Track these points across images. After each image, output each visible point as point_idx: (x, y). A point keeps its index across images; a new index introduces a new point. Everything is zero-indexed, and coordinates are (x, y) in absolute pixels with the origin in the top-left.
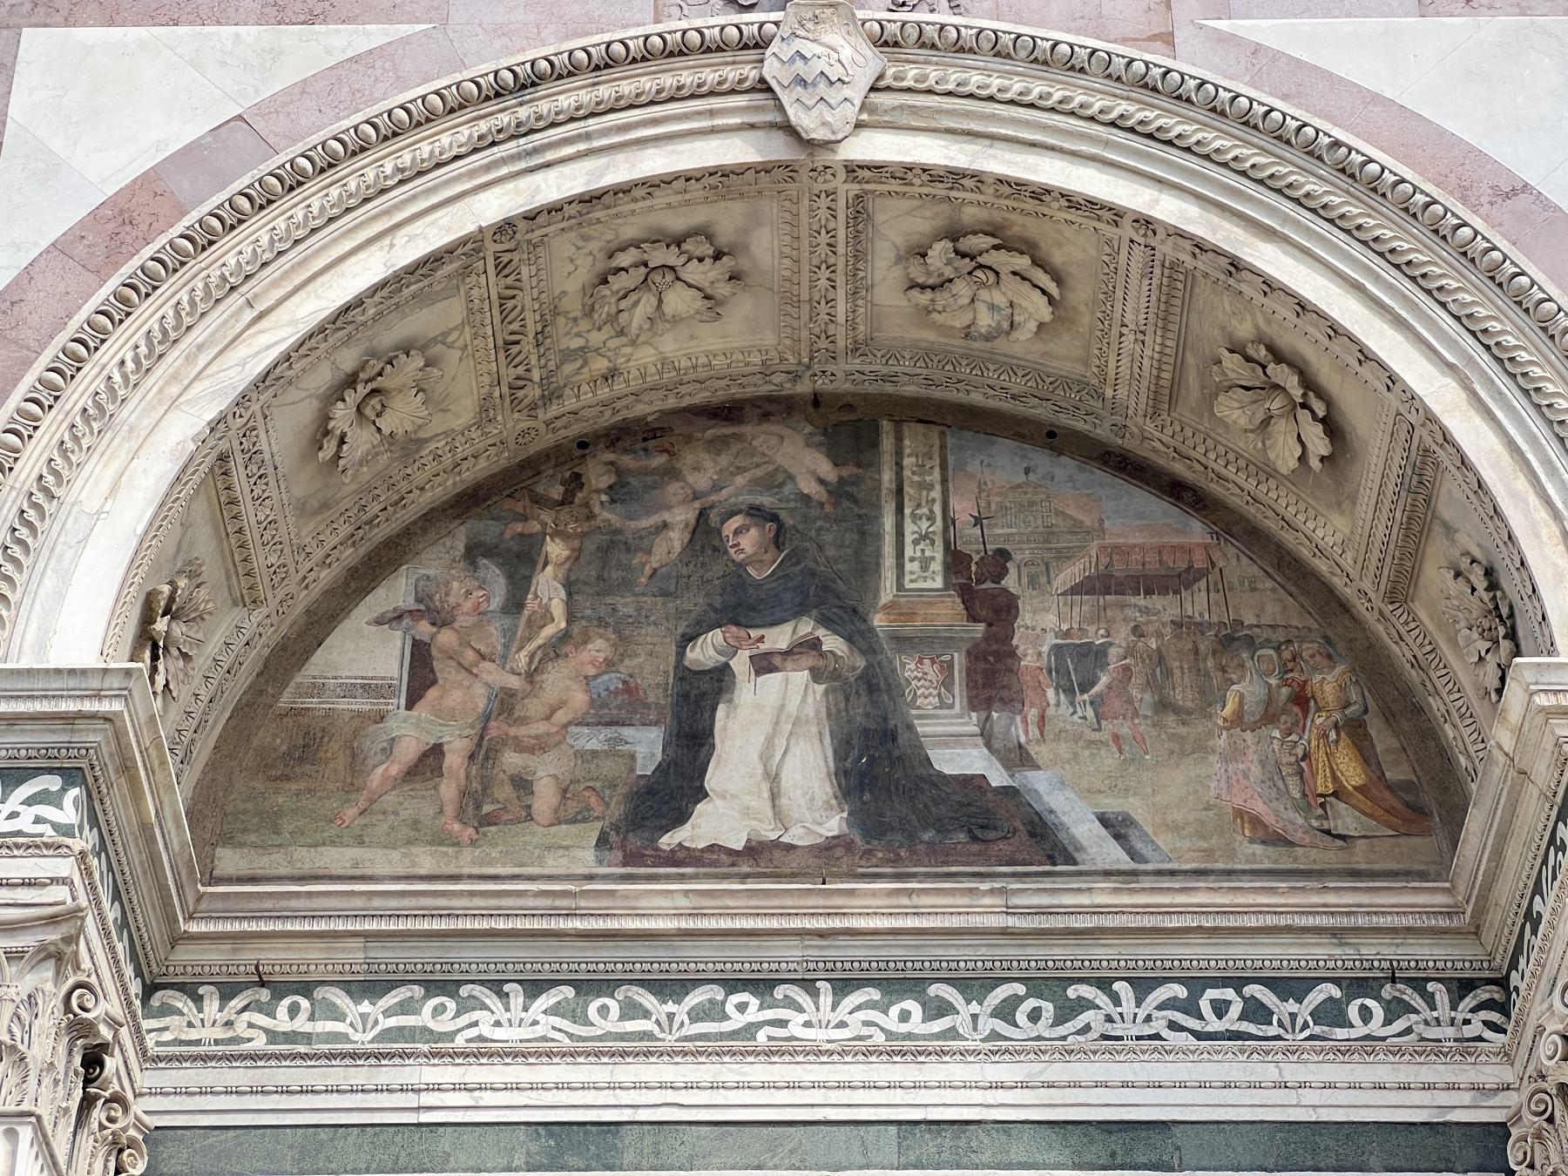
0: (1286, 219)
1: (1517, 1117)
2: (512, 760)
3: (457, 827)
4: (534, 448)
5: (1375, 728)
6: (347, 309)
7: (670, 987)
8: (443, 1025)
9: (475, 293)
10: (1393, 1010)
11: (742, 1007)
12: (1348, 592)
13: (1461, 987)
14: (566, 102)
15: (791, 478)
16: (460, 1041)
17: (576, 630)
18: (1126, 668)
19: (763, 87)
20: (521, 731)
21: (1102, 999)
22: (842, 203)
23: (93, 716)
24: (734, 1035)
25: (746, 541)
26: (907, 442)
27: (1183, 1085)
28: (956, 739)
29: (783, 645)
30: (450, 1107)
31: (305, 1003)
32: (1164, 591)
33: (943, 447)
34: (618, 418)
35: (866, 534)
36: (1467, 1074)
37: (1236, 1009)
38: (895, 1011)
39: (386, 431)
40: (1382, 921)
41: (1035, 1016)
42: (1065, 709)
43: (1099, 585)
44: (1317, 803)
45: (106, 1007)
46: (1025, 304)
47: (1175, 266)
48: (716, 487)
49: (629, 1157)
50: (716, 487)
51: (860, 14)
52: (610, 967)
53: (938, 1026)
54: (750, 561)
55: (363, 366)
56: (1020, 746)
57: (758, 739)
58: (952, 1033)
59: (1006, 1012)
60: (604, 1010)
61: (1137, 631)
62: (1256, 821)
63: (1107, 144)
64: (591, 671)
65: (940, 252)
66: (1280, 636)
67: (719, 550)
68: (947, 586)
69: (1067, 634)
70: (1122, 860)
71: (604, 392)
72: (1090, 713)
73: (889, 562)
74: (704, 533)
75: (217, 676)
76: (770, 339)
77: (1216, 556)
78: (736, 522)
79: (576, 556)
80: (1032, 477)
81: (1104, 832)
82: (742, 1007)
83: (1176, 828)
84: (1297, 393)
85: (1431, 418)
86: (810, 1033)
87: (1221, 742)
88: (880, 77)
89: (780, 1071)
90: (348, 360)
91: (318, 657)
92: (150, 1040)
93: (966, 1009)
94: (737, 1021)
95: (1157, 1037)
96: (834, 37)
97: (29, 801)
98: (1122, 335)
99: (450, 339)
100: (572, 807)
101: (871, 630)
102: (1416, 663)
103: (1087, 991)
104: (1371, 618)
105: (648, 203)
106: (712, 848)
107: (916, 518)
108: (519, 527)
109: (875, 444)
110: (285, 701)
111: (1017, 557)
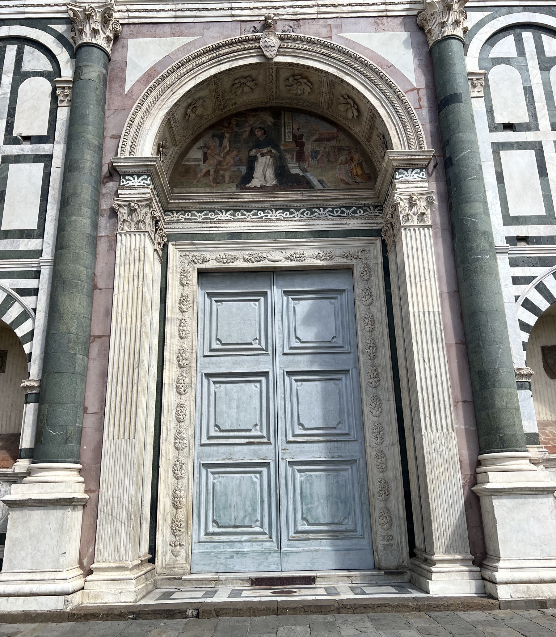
0: (351, 72)
1: (383, 228)
2: (221, 172)
4: (223, 117)
5: (364, 164)
6: (189, 91)
7: (249, 211)
10: (365, 211)
11: (260, 213)
12: (360, 140)
13: (375, 207)
14: (225, 51)
15: (266, 122)
16: (215, 220)
17: (231, 149)
19: (259, 47)
21: (318, 211)
23: (151, 165)
24: (259, 218)
25: (259, 133)
27: (331, 224)
28: (294, 168)
29: (266, 152)
30: (214, 230)
35: (279, 132)
36: (376, 221)
37: (339, 212)
40: (363, 197)
41: (307, 214)
42: (312, 162)
43: (318, 140)
44: (354, 177)
45: (158, 214)
47: (332, 81)
48: (254, 124)
49: (243, 238)
50: (254, 124)
51: (277, 33)
53: (292, 216)
55: (192, 102)
57: (262, 168)
58: (294, 217)
59: (303, 213)
61: (325, 148)
62: (344, 180)
63: (320, 58)
65: (291, 79)
66: (348, 148)
67: (255, 135)
70: (322, 188)
71: (234, 107)
73: (283, 136)
74: (252, 132)
75: (171, 158)
78: (257, 130)
79: (231, 136)
82: (260, 213)
83: (331, 182)
84: (352, 104)
85: (375, 108)
87: (338, 167)
88: (280, 45)
89: (267, 224)
90: (189, 101)
91: (188, 155)
92: (166, 220)
94: (260, 216)
96: (272, 38)
97: (142, 180)
100: (232, 180)
102: (371, 153)
103: (316, 210)
104: (363, 145)
106: (255, 187)
107: (288, 129)
109: (281, 115)
110: (183, 163)
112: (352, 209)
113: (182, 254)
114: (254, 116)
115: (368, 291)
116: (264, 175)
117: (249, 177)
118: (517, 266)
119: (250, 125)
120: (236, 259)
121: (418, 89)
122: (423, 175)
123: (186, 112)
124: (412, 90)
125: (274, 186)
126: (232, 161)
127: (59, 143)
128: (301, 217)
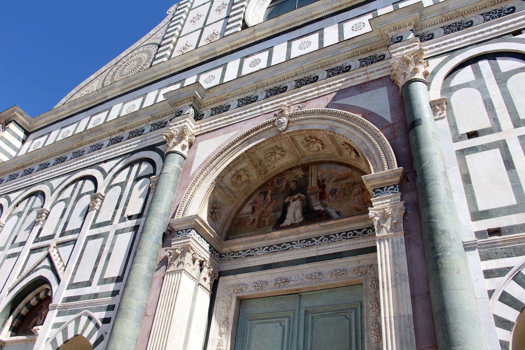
2: (263, 219)
3: (256, 229)
8: (253, 254)
11: (288, 246)
15: (298, 176)
18: (340, 191)
21: (334, 236)
24: (287, 249)
26: (313, 167)
28: (317, 205)
29: (296, 197)
30: (253, 264)
31: (237, 254)
32: (345, 179)
33: (317, 167)
34: (277, 173)
37: (352, 235)
38: (307, 243)
41: (325, 240)
48: (289, 179)
50: (289, 179)
53: (312, 244)
56: (326, 204)
57: (292, 210)
58: (314, 245)
61: (342, 186)
62: (357, 208)
64: (273, 206)
68: (317, 185)
69: (332, 188)
71: (273, 170)
72: (335, 198)
74: (288, 185)
76: (292, 158)
78: (291, 183)
79: (272, 191)
80: (329, 168)
81: (336, 213)
86: (296, 248)
93: (316, 241)
94: (287, 247)
95: (341, 240)
99: (248, 167)
101: (307, 193)
103: (332, 236)
105: (264, 144)
108: (266, 189)
109: (309, 169)
110: (238, 217)
111: (326, 179)
112: (363, 231)
114: (289, 173)
115: (375, 303)
116: (294, 215)
117: (283, 218)
118: (490, 259)
119: (287, 180)
121: (393, 124)
122: (396, 190)
124: (387, 126)
125: (301, 222)
126: (272, 209)
127: (144, 217)
128: (320, 244)
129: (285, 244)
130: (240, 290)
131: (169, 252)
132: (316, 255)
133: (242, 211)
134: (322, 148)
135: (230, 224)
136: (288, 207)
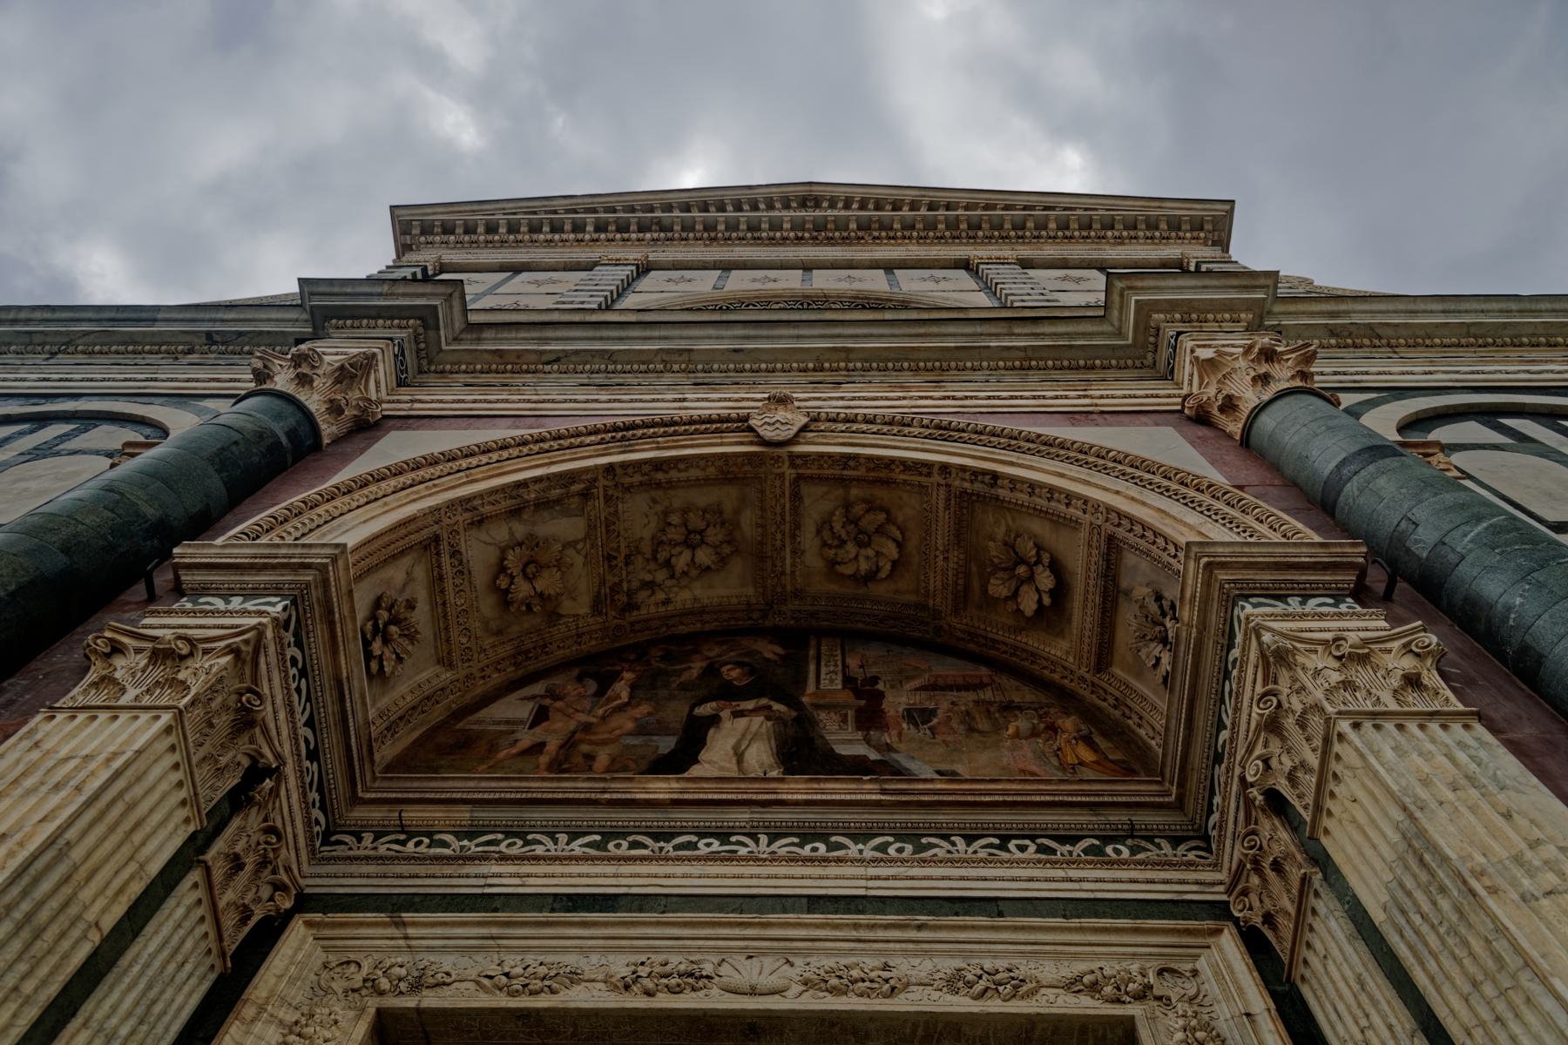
5: (1098, 739)
9: (592, 513)
17: (633, 702)
20: (593, 738)
22: (787, 483)
31: (426, 841)
37: (1032, 848)
39: (539, 590)
46: (885, 551)
52: (626, 824)
54: (735, 679)
57: (732, 741)
60: (618, 846)
68: (844, 687)
72: (928, 732)
77: (996, 678)
78: (729, 667)
82: (708, 845)
98: (936, 556)
99: (580, 546)
104: (1086, 694)
113: (333, 959)
119: (708, 658)
120: (574, 978)
123: (503, 559)
129: (694, 839)
130: (403, 986)
131: (111, 640)
132: (862, 892)
133: (484, 713)
134: (895, 564)
135: (414, 742)
136: (711, 731)
